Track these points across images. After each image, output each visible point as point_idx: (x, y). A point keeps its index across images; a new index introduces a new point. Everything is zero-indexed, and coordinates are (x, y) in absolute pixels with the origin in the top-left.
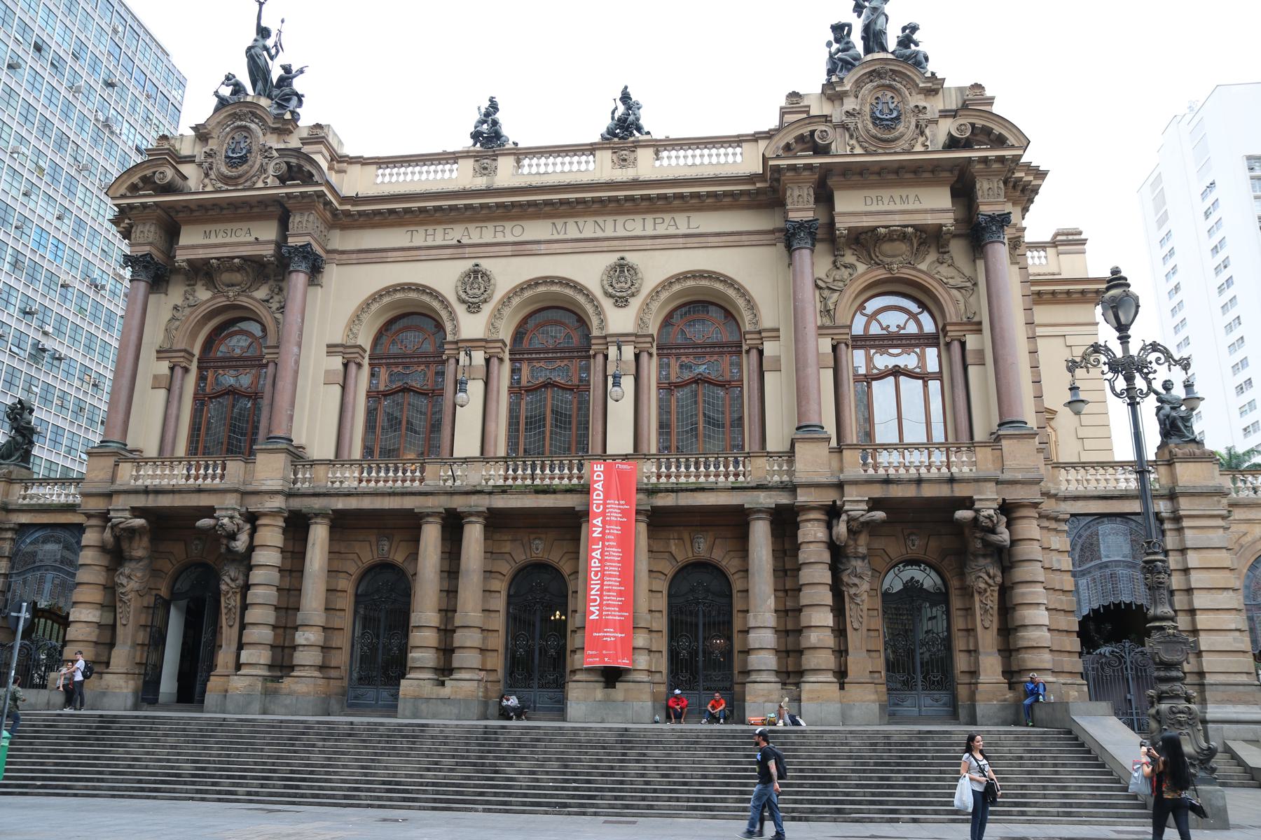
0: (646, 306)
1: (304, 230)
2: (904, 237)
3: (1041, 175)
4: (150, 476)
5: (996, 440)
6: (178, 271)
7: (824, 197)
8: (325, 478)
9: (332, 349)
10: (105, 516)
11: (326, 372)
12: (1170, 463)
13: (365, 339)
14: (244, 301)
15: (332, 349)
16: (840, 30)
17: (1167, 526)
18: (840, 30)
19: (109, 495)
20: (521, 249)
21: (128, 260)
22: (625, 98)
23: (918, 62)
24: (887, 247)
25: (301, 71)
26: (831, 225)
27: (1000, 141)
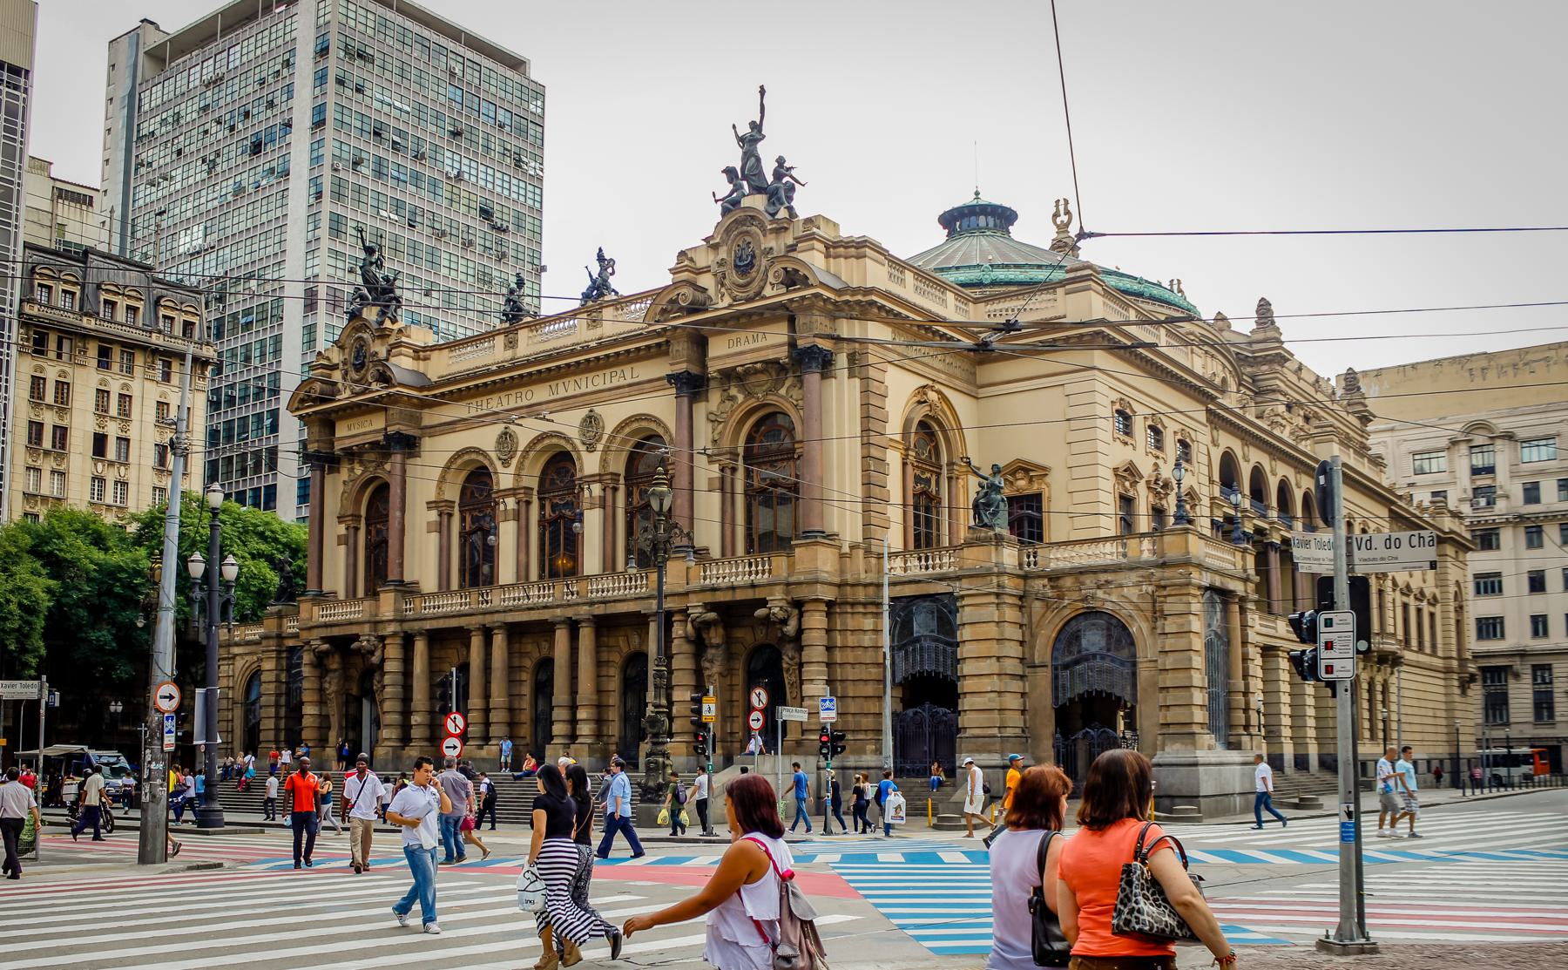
2: (762, 372)
8: (428, 608)
9: (431, 505)
13: (453, 493)
15: (431, 505)
20: (532, 410)
24: (753, 379)
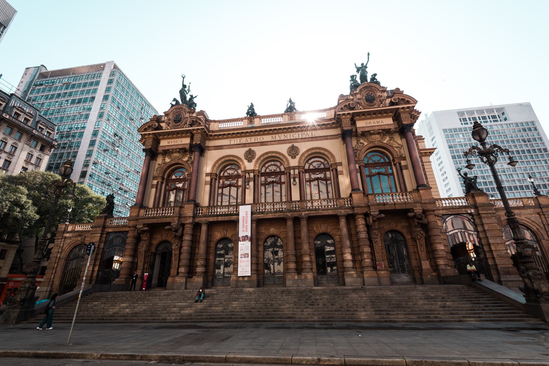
0: (301, 158)
2: (379, 133)
3: (419, 113)
4: (151, 213)
5: (417, 190)
7: (353, 122)
10: (135, 227)
12: (473, 197)
15: (207, 175)
16: (352, 77)
19: (137, 220)
20: (263, 144)
21: (144, 150)
22: (290, 101)
23: (378, 83)
26: (356, 131)
27: (408, 102)
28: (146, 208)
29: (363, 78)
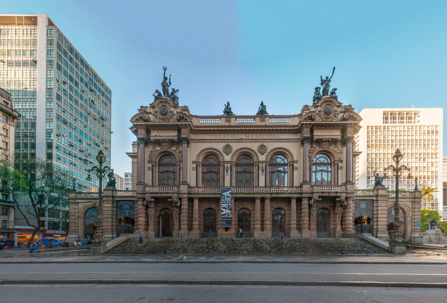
0: (268, 155)
1: (185, 133)
6: (151, 142)
9: (193, 162)
11: (193, 168)
12: (377, 190)
14: (169, 150)
15: (193, 162)
17: (375, 202)
18: (317, 89)
20: (238, 141)
25: (178, 91)
28: (145, 186)
29: (325, 91)
